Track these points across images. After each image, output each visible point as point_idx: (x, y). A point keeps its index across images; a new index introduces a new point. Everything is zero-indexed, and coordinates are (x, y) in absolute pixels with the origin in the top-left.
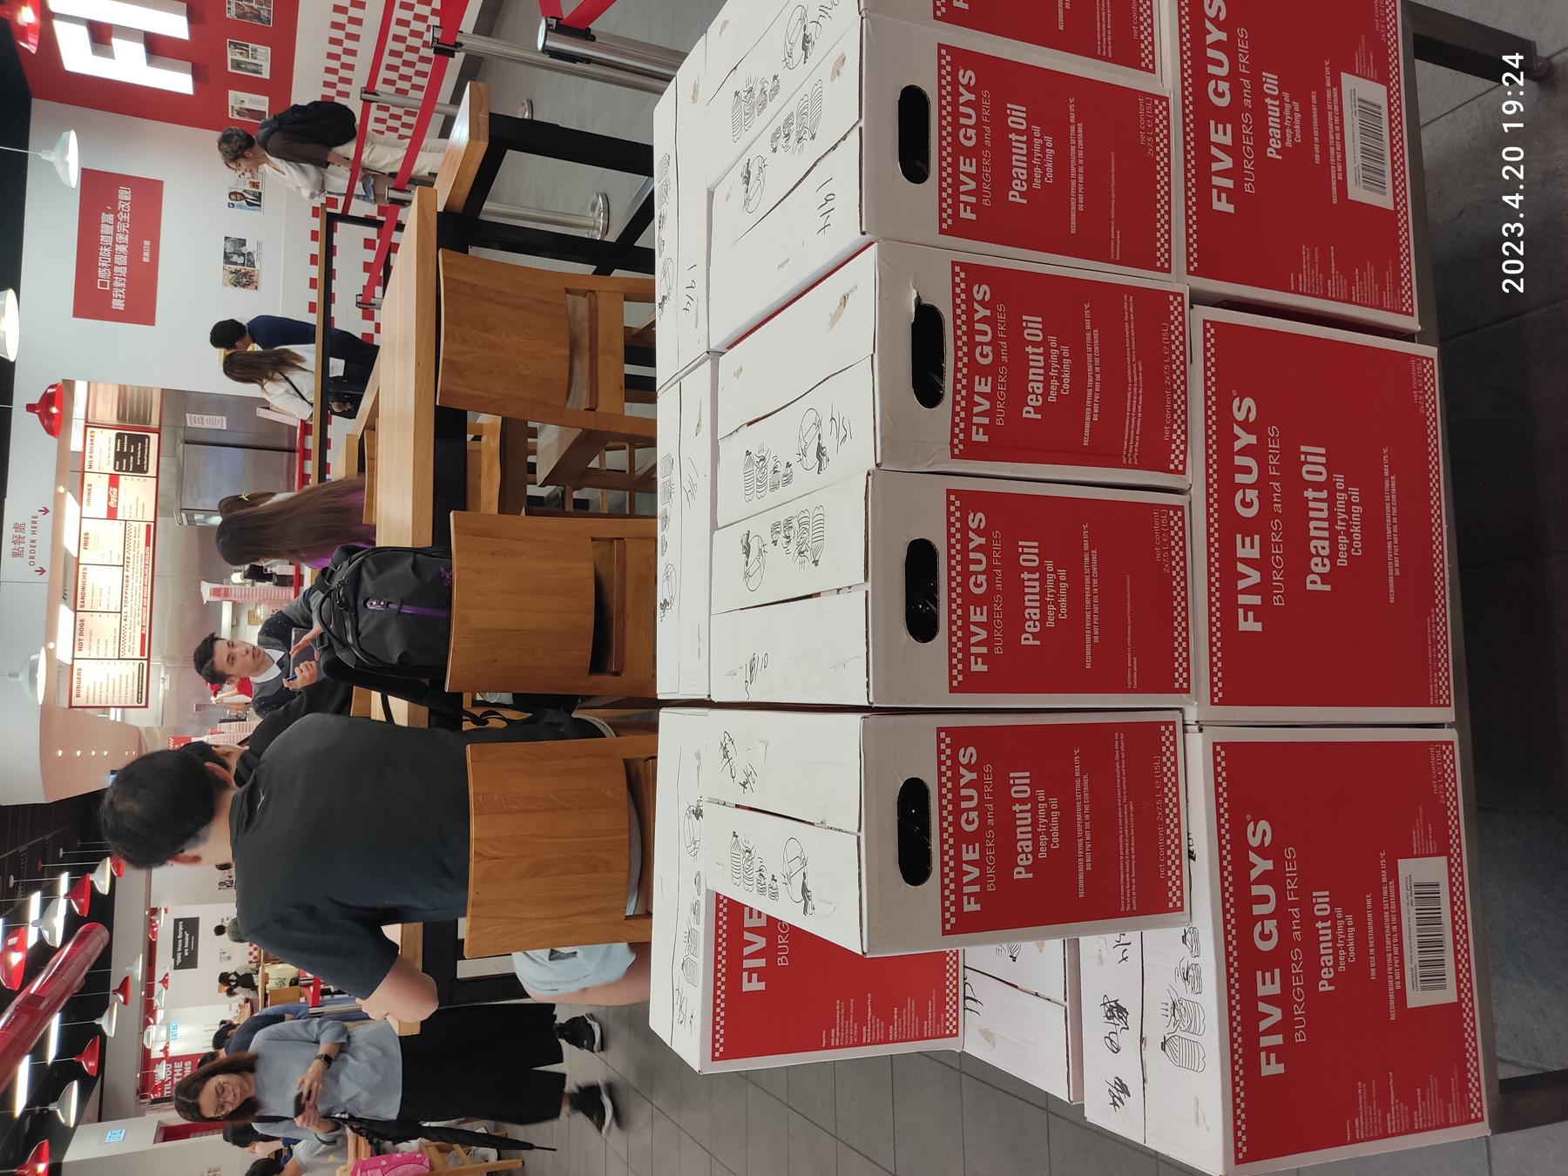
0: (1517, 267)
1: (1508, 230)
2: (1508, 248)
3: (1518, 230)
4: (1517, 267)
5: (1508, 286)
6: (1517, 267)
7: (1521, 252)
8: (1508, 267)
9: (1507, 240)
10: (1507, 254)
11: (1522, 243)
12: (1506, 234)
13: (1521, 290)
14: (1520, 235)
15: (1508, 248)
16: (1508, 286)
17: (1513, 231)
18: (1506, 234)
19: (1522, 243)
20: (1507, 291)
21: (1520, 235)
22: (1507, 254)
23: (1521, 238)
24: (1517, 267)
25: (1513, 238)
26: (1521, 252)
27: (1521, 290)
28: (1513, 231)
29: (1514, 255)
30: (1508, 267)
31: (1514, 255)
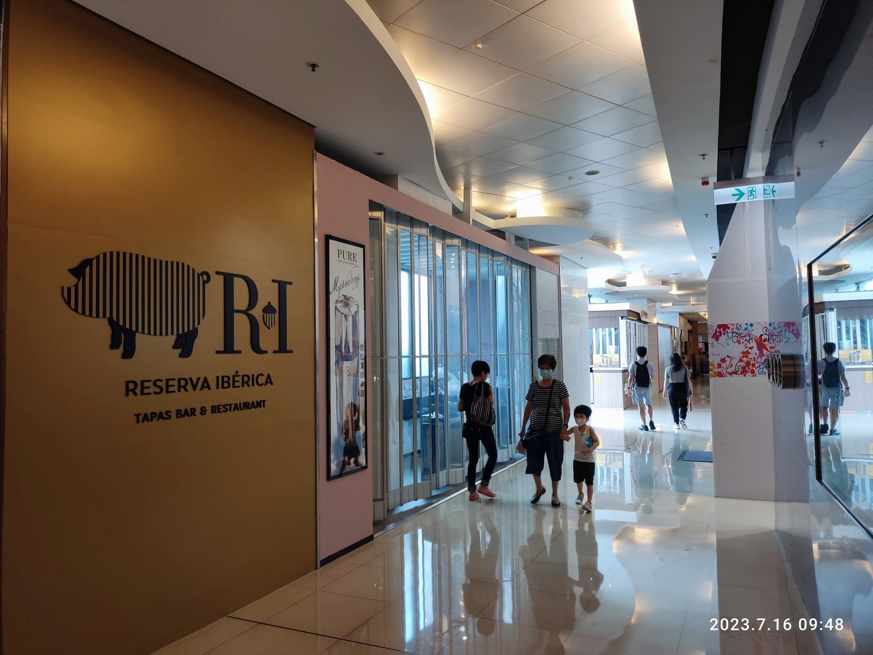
0: (724, 627)
1: (745, 622)
2: (735, 622)
3: (745, 627)
4: (724, 627)
5: (714, 622)
6: (724, 627)
7: (733, 629)
8: (724, 622)
9: (740, 621)
10: (732, 621)
11: (738, 629)
12: (742, 620)
13: (712, 629)
14: (742, 628)
15: (735, 622)
16: (714, 622)
17: (744, 624)
18: (742, 620)
19: (738, 629)
20: (711, 621)
21: (742, 628)
22: (732, 621)
23: (740, 629)
24: (724, 627)
25: (741, 624)
26: (733, 629)
27: (712, 629)
28: (744, 624)
29: (731, 625)
30: (724, 622)
31: (731, 625)
